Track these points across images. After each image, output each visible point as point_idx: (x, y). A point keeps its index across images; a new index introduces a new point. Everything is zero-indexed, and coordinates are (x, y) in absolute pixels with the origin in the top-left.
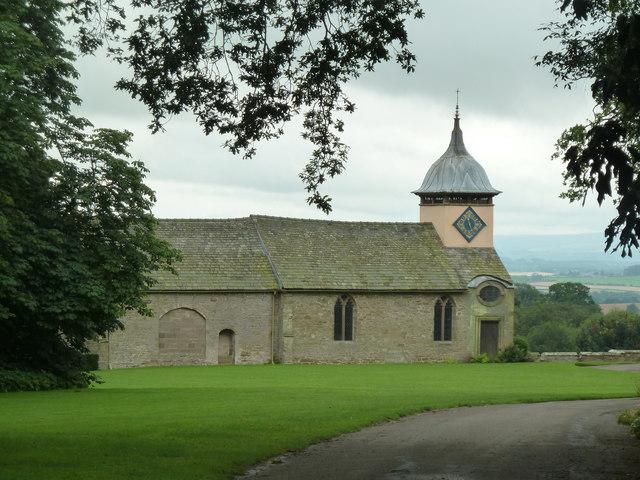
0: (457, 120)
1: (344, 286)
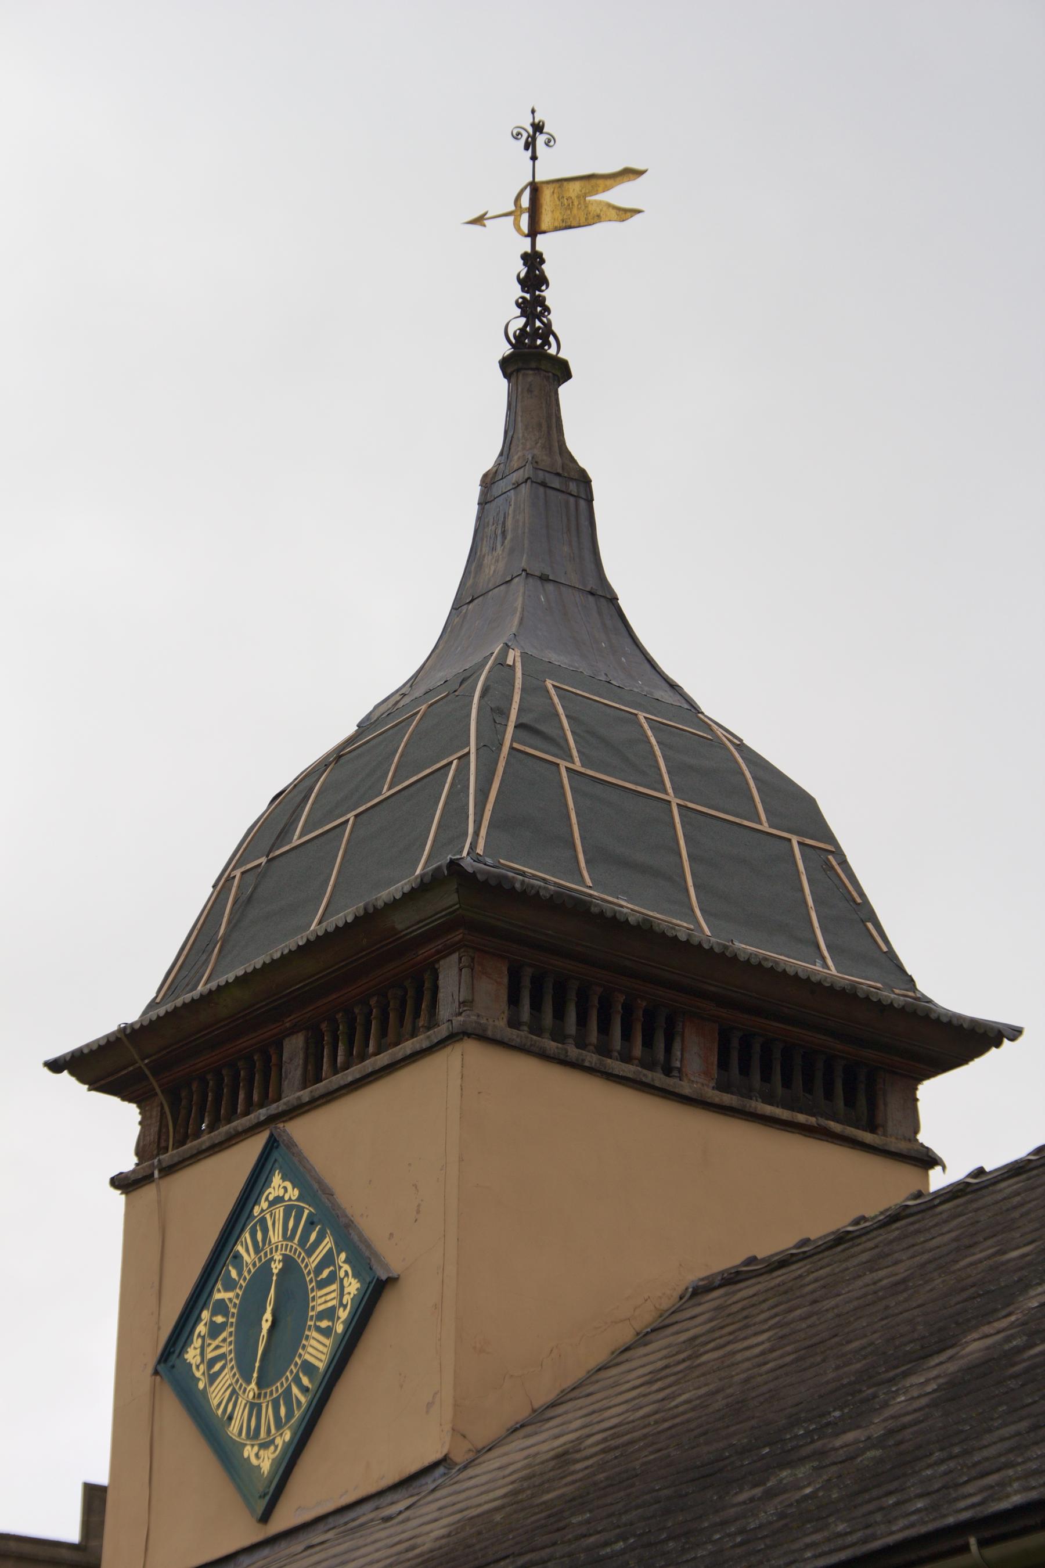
0: (534, 364)
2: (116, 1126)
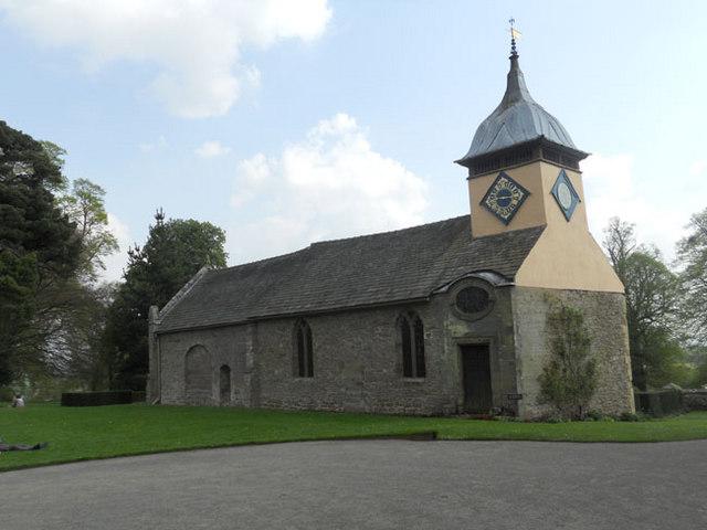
0: (514, 58)
1: (298, 308)
2: (465, 171)
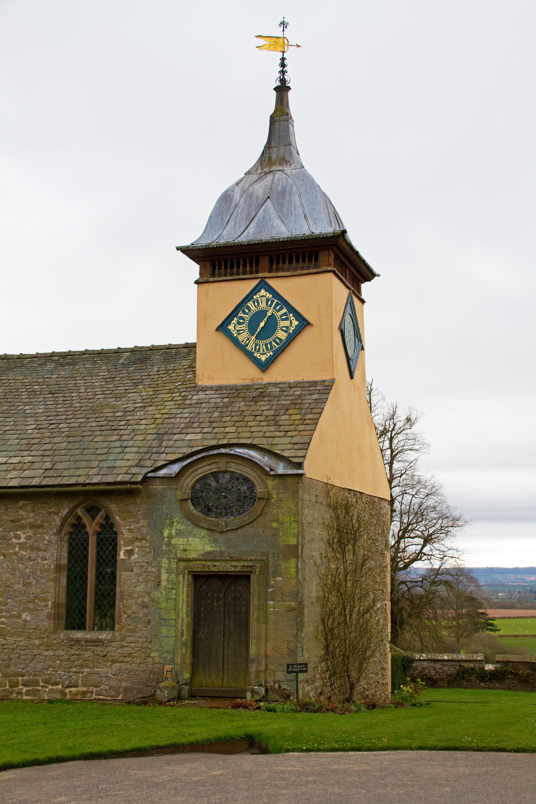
0: (282, 89)
